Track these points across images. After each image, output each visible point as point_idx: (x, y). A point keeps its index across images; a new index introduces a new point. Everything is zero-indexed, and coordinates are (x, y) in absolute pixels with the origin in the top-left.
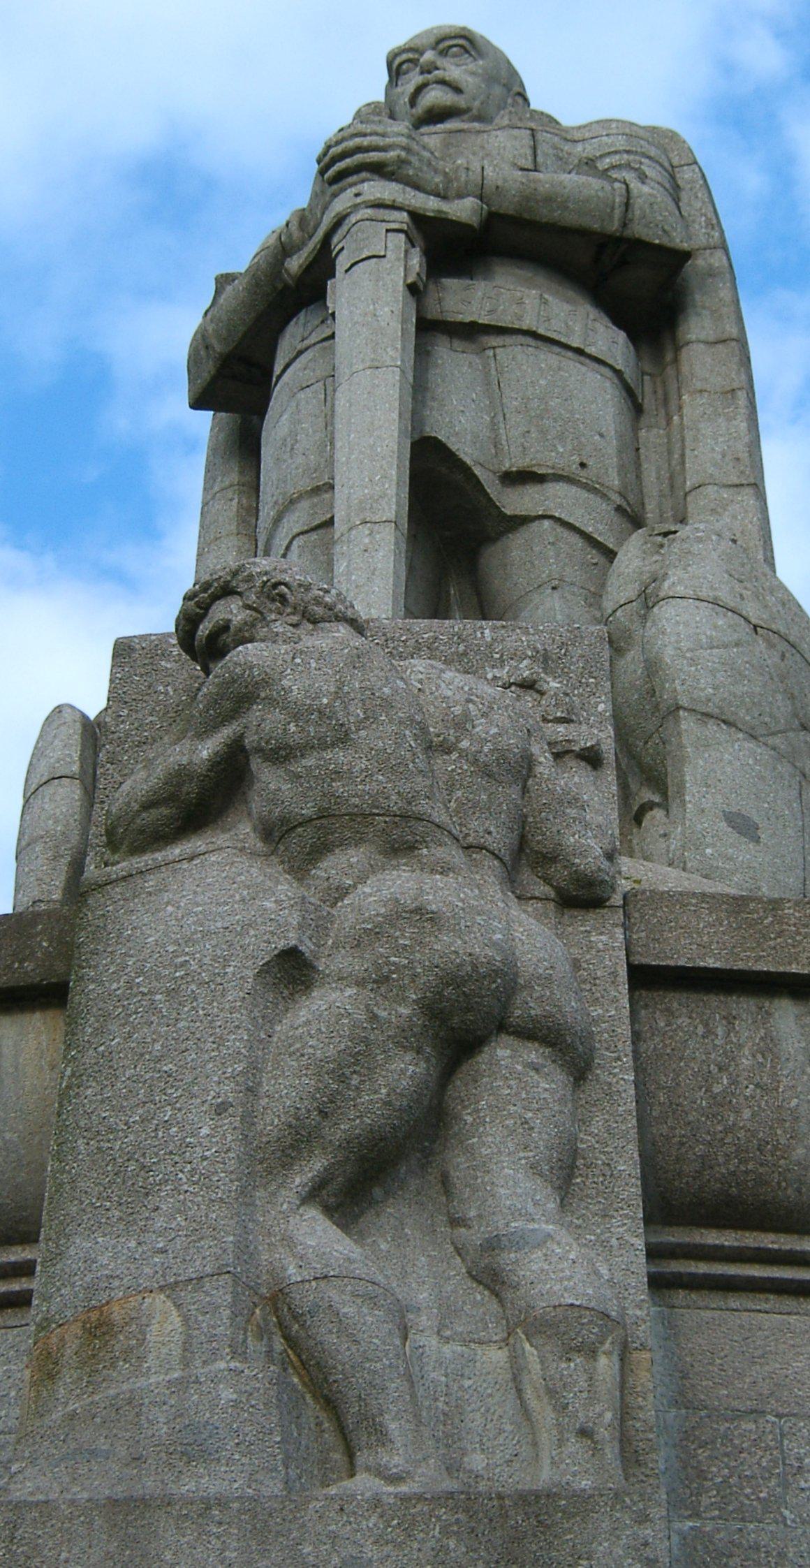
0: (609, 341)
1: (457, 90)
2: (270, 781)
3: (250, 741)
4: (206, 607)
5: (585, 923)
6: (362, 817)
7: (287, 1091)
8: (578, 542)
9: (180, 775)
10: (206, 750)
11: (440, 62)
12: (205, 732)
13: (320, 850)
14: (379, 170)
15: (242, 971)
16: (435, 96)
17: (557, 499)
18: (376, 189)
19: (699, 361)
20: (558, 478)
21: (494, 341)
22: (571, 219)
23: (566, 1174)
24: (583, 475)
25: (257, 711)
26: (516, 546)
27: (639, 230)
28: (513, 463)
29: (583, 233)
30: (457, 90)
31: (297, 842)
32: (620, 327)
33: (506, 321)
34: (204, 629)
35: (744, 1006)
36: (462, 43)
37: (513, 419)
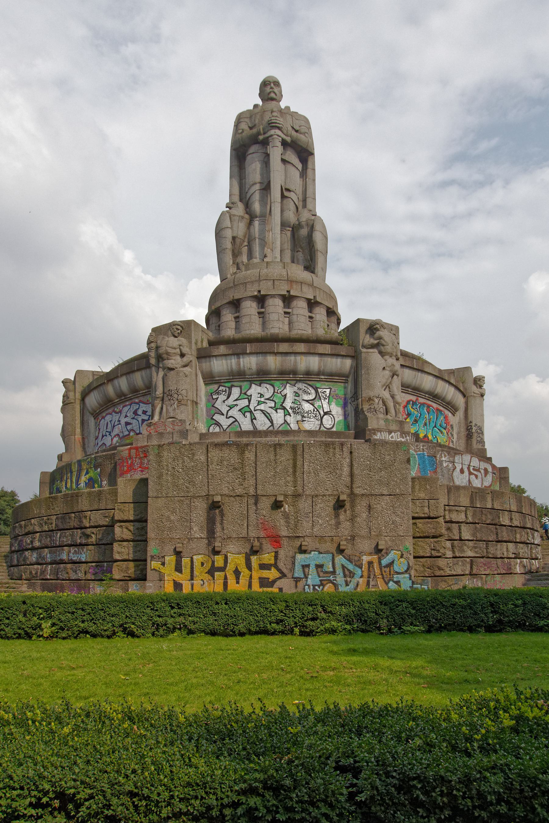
0: (300, 166)
1: (276, 95)
7: (384, 381)
11: (274, 87)
16: (272, 95)
17: (292, 195)
19: (309, 171)
21: (287, 164)
22: (301, 144)
24: (295, 191)
28: (287, 187)
29: (301, 147)
30: (276, 95)
33: (290, 161)
36: (277, 84)
37: (288, 179)
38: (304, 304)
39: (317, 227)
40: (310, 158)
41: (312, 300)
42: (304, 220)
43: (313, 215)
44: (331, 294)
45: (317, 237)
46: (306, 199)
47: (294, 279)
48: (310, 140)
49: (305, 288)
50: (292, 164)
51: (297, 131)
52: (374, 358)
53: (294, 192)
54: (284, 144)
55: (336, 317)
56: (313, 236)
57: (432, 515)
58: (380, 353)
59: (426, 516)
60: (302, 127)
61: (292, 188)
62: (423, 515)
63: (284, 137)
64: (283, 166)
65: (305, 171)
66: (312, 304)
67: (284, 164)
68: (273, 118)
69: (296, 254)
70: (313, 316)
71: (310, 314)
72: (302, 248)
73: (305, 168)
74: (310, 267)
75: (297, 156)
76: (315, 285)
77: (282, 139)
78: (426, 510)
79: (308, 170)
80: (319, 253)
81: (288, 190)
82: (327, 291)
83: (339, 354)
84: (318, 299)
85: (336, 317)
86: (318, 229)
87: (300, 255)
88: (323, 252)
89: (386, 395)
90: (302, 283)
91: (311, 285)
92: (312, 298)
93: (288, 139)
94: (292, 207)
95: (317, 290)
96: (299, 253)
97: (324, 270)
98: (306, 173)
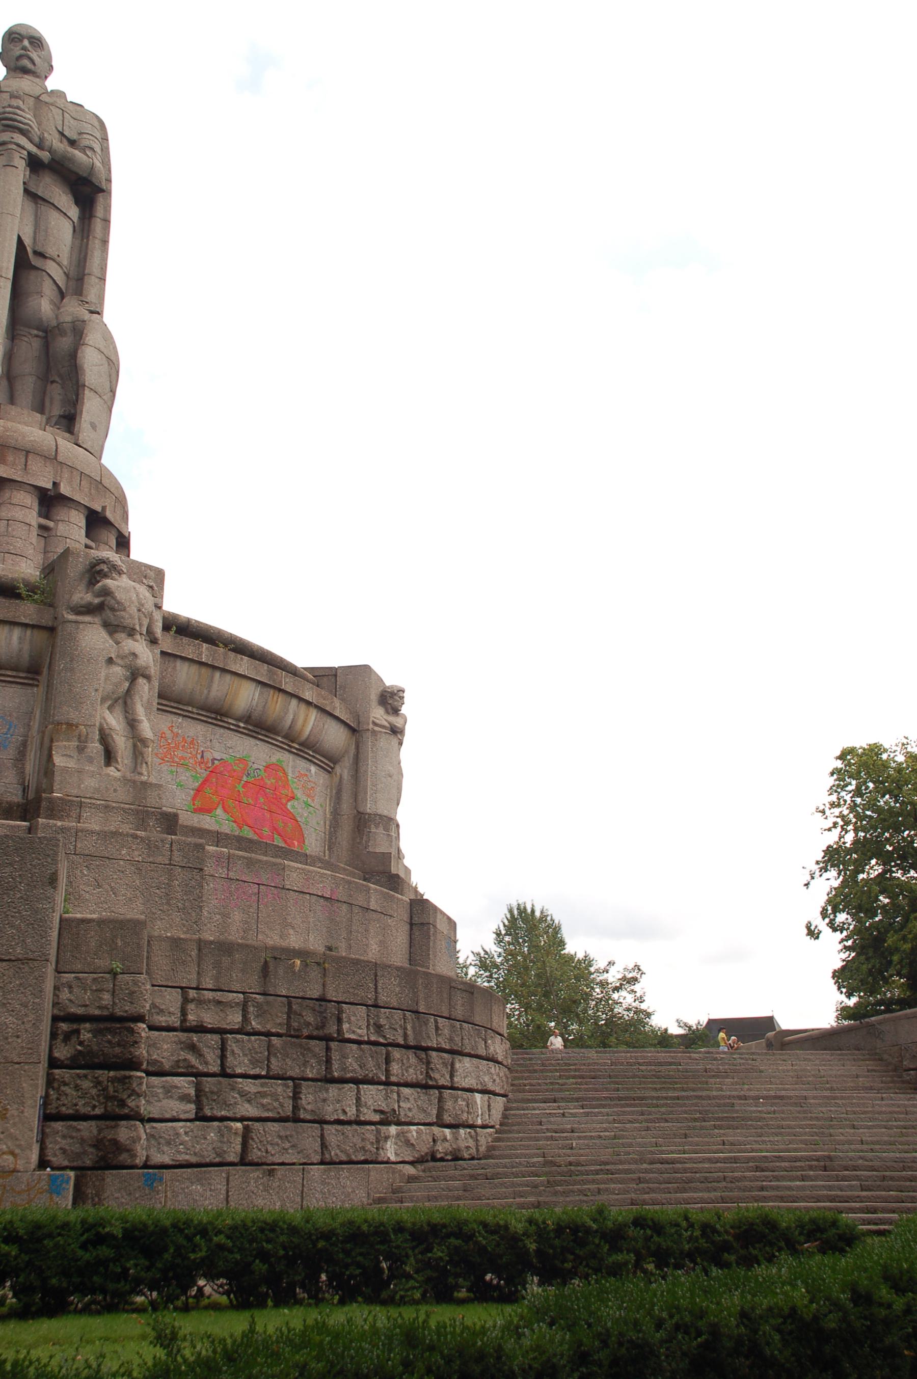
0: (74, 212)
2: (108, 613)
3: (106, 603)
4: (99, 564)
5: (155, 646)
6: (125, 627)
8: (51, 282)
9: (90, 604)
10: (97, 601)
12: (98, 596)
13: (116, 632)
14: (23, 133)
15: (102, 660)
18: (23, 141)
19: (98, 225)
20: (51, 259)
21: (40, 202)
22: (75, 169)
23: (148, 708)
24: (58, 259)
25: (109, 598)
26: (33, 275)
27: (94, 180)
28: (39, 249)
29: (77, 174)
31: (112, 628)
32: (77, 203)
34: (98, 568)
35: (172, 659)
38: (30, 500)
39: (92, 337)
40: (100, 198)
41: (49, 490)
42: (68, 319)
43: (92, 312)
44: (106, 482)
45: (90, 359)
46: (83, 277)
47: (12, 443)
48: (98, 164)
49: (35, 464)
50: (53, 205)
51: (72, 143)
52: (93, 638)
53: (54, 260)
54: (35, 164)
55: (114, 532)
56: (79, 355)
57: (119, 1012)
58: (106, 625)
59: (106, 1013)
60: (85, 136)
61: (51, 251)
62: (97, 1012)
63: (34, 150)
64: (30, 206)
65: (86, 221)
66: (50, 501)
67: (36, 203)
68: (8, 110)
69: (49, 387)
70: (51, 524)
71: (43, 521)
72: (60, 376)
73: (87, 216)
74: (68, 421)
75: (68, 191)
76: (60, 459)
77: (29, 153)
78: (107, 997)
79: (93, 220)
80: (87, 391)
81: (41, 255)
82: (92, 475)
83: (17, 620)
84: (64, 490)
85: (114, 532)
86: (91, 343)
87: (56, 392)
88: (100, 390)
89: (114, 721)
90: (28, 452)
91: (53, 458)
92: (49, 486)
93: (45, 156)
94: (48, 289)
95: (65, 470)
96: (55, 385)
97: (102, 429)
98: (89, 225)
